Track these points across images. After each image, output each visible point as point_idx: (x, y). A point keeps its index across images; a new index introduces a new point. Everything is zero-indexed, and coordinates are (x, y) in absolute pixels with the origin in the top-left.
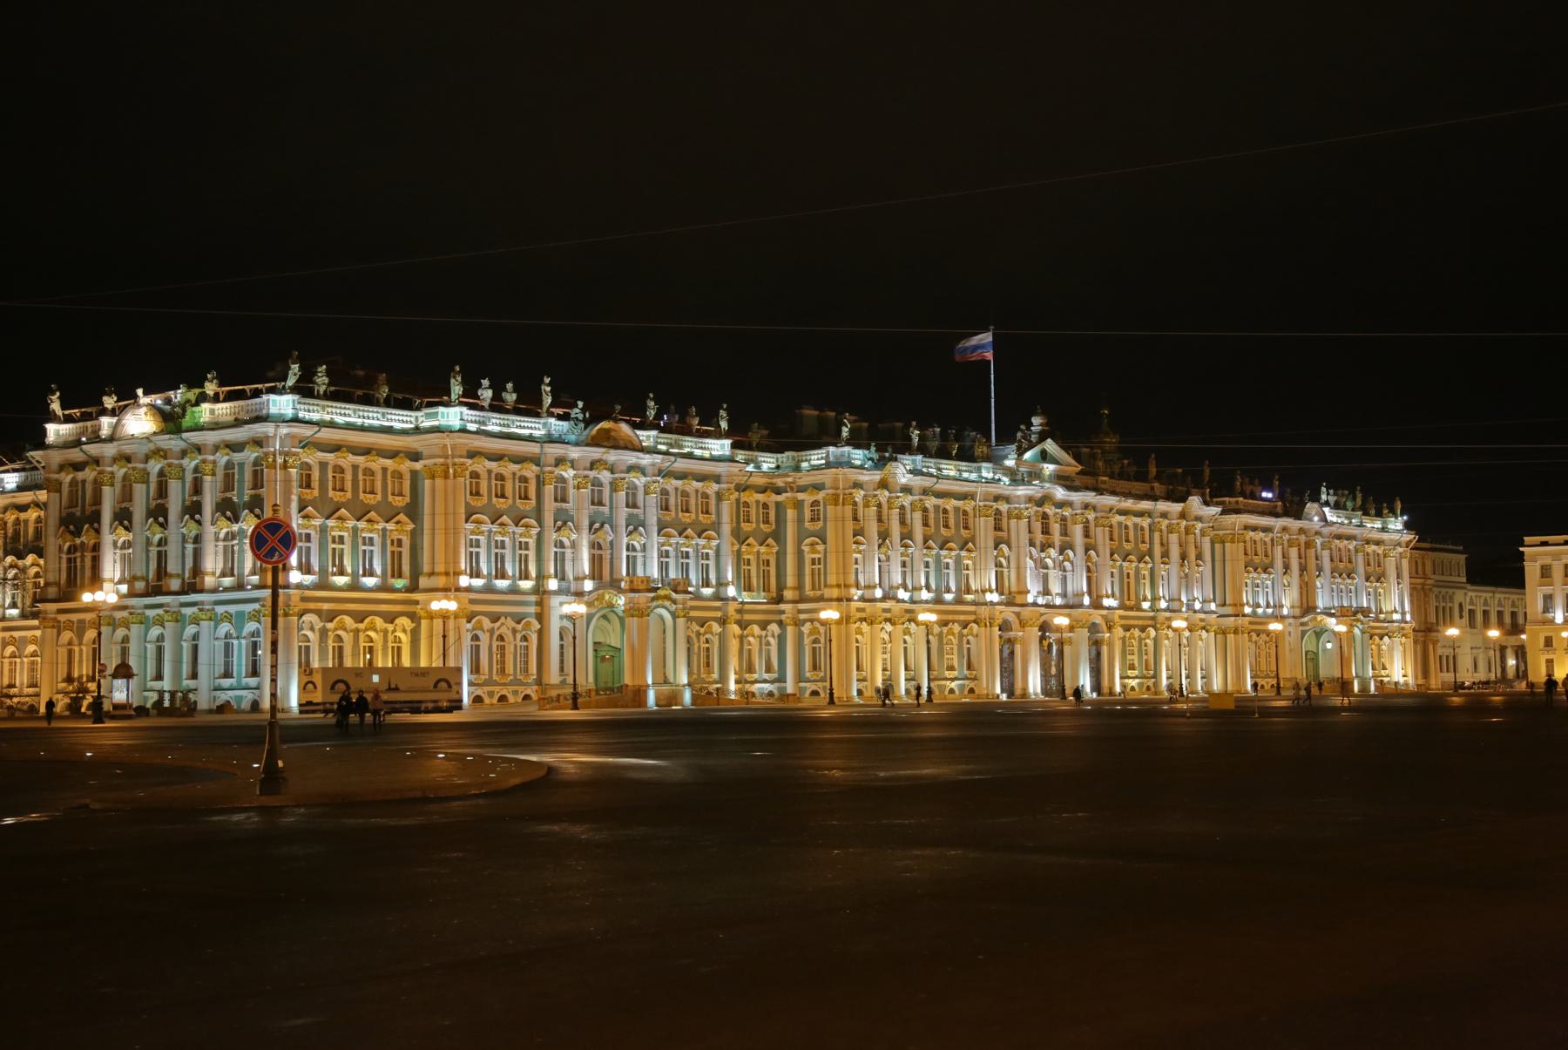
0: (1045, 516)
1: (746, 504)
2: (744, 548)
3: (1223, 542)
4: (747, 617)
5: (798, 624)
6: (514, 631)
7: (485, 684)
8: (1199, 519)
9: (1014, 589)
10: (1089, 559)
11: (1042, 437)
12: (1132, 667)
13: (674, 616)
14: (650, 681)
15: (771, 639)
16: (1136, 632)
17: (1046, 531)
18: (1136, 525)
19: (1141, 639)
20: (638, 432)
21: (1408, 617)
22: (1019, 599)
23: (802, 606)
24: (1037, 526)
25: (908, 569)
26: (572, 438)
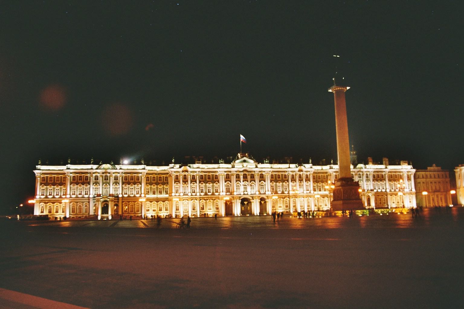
2: (158, 186)
4: (159, 200)
9: (232, 191)
26: (111, 168)
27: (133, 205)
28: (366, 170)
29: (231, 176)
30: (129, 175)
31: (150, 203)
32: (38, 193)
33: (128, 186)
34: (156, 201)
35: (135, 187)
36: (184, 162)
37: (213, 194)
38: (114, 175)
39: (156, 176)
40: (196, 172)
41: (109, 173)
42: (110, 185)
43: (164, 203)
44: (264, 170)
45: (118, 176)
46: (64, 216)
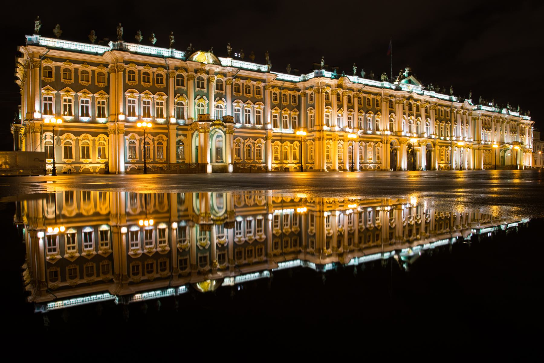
0: (410, 104)
1: (284, 95)
2: (283, 112)
4: (284, 138)
6: (153, 140)
7: (137, 163)
8: (468, 110)
10: (427, 121)
12: (442, 160)
13: (225, 133)
14: (209, 161)
15: (296, 147)
16: (444, 148)
17: (410, 109)
18: (445, 110)
19: (446, 150)
20: (220, 58)
22: (399, 134)
24: (407, 108)
27: (249, 146)
28: (507, 116)
29: (395, 104)
30: (244, 81)
34: (280, 141)
36: (341, 68)
37: (374, 134)
39: (279, 91)
43: (292, 145)
45: (222, 82)
46: (103, 166)
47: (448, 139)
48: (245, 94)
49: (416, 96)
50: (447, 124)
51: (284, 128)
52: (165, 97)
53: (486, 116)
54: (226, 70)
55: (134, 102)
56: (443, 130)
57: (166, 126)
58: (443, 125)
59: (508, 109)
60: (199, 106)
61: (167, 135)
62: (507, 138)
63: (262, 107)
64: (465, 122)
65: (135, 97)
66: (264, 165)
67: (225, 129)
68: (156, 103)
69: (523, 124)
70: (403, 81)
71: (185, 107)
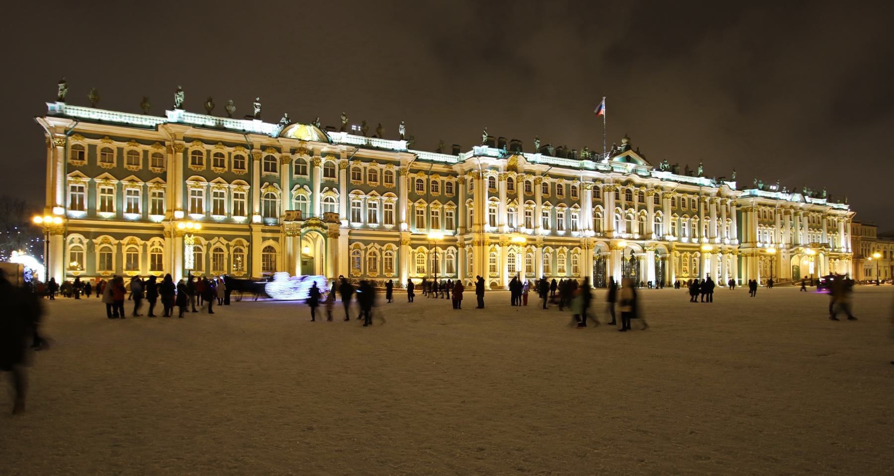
0: (628, 191)
1: (435, 182)
2: (431, 205)
3: (746, 212)
5: (463, 246)
6: (228, 246)
8: (728, 197)
11: (628, 148)
16: (689, 254)
17: (629, 198)
18: (689, 199)
21: (850, 250)
22: (608, 235)
23: (466, 236)
24: (623, 197)
25: (532, 217)
27: (375, 254)
28: (802, 205)
30: (367, 164)
31: (411, 250)
32: (59, 200)
33: (363, 197)
35: (381, 200)
37: (568, 234)
38: (324, 160)
39: (426, 176)
40: (534, 174)
41: (311, 153)
42: (312, 190)
43: (446, 251)
44: (662, 184)
45: (334, 166)
47: (695, 240)
48: (368, 182)
49: (637, 180)
50: (692, 219)
51: (433, 228)
52: (247, 187)
53: (765, 205)
54: (338, 149)
55: (200, 193)
56: (686, 228)
57: (247, 227)
58: (685, 220)
59: (804, 195)
60: (298, 198)
61: (249, 239)
62: (803, 237)
63: (395, 199)
64: (724, 215)
65: (202, 187)
66: (397, 279)
67: (325, 231)
68: (233, 195)
69: (835, 215)
70: (616, 159)
71: (278, 200)
